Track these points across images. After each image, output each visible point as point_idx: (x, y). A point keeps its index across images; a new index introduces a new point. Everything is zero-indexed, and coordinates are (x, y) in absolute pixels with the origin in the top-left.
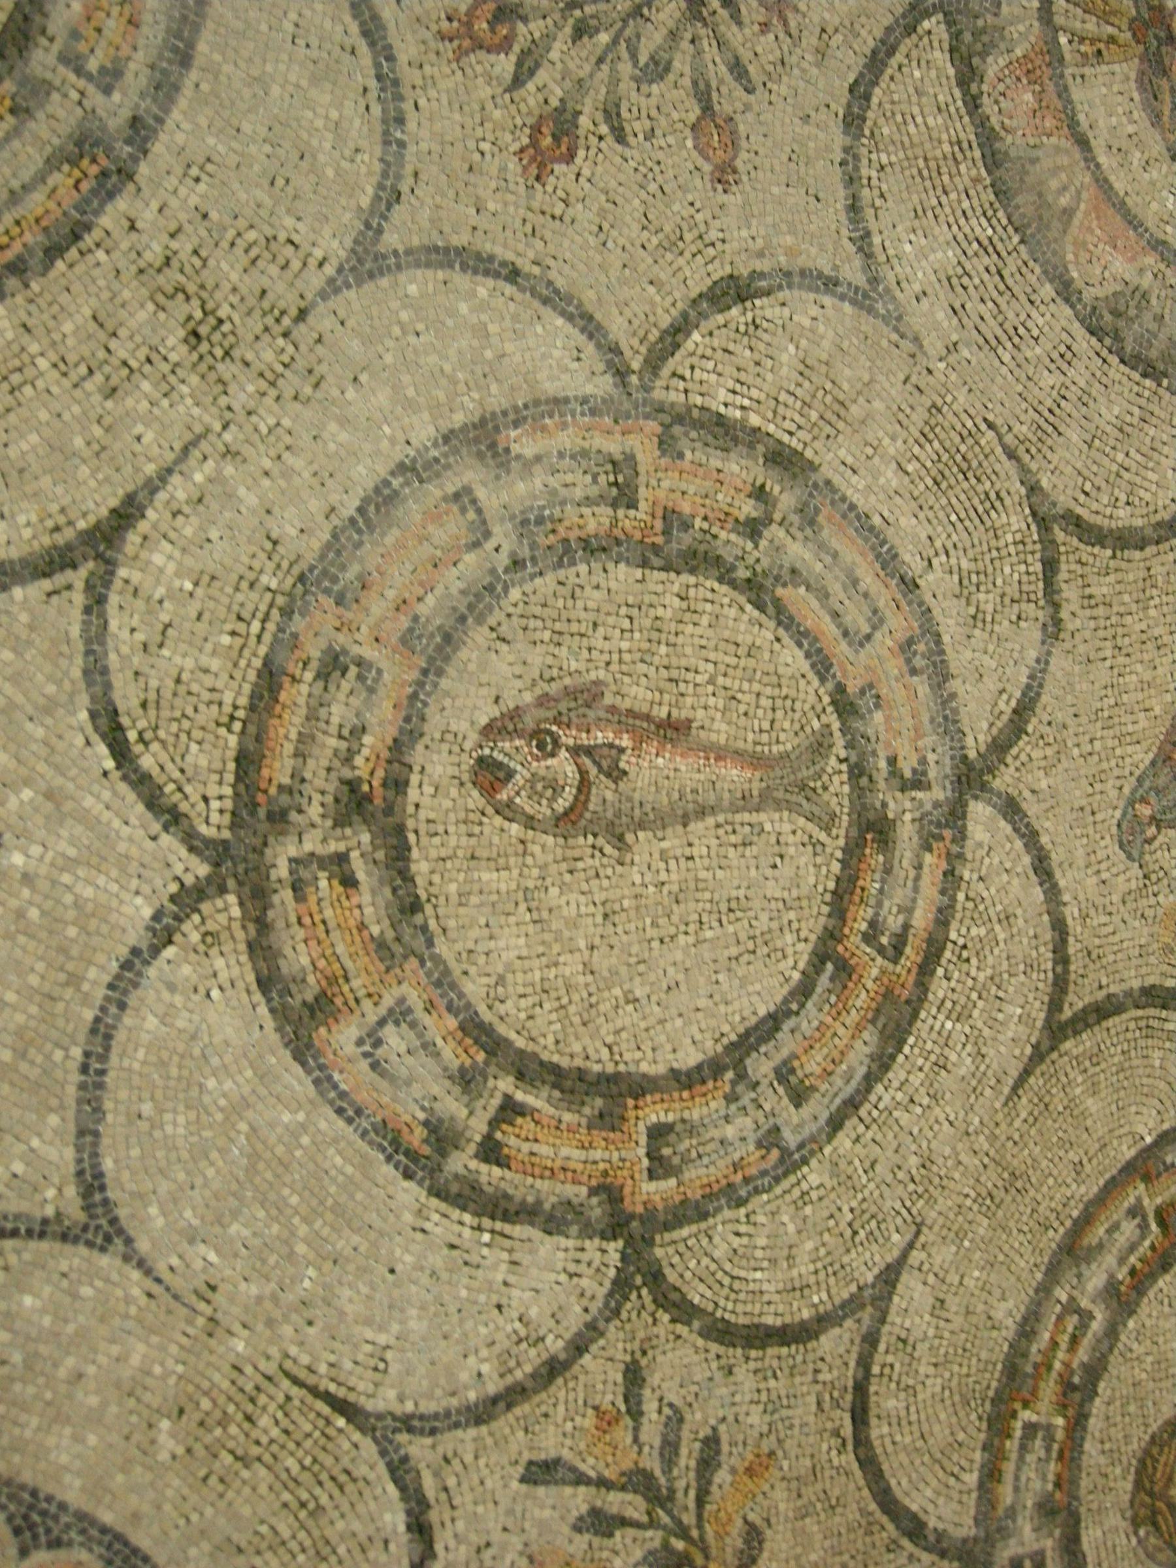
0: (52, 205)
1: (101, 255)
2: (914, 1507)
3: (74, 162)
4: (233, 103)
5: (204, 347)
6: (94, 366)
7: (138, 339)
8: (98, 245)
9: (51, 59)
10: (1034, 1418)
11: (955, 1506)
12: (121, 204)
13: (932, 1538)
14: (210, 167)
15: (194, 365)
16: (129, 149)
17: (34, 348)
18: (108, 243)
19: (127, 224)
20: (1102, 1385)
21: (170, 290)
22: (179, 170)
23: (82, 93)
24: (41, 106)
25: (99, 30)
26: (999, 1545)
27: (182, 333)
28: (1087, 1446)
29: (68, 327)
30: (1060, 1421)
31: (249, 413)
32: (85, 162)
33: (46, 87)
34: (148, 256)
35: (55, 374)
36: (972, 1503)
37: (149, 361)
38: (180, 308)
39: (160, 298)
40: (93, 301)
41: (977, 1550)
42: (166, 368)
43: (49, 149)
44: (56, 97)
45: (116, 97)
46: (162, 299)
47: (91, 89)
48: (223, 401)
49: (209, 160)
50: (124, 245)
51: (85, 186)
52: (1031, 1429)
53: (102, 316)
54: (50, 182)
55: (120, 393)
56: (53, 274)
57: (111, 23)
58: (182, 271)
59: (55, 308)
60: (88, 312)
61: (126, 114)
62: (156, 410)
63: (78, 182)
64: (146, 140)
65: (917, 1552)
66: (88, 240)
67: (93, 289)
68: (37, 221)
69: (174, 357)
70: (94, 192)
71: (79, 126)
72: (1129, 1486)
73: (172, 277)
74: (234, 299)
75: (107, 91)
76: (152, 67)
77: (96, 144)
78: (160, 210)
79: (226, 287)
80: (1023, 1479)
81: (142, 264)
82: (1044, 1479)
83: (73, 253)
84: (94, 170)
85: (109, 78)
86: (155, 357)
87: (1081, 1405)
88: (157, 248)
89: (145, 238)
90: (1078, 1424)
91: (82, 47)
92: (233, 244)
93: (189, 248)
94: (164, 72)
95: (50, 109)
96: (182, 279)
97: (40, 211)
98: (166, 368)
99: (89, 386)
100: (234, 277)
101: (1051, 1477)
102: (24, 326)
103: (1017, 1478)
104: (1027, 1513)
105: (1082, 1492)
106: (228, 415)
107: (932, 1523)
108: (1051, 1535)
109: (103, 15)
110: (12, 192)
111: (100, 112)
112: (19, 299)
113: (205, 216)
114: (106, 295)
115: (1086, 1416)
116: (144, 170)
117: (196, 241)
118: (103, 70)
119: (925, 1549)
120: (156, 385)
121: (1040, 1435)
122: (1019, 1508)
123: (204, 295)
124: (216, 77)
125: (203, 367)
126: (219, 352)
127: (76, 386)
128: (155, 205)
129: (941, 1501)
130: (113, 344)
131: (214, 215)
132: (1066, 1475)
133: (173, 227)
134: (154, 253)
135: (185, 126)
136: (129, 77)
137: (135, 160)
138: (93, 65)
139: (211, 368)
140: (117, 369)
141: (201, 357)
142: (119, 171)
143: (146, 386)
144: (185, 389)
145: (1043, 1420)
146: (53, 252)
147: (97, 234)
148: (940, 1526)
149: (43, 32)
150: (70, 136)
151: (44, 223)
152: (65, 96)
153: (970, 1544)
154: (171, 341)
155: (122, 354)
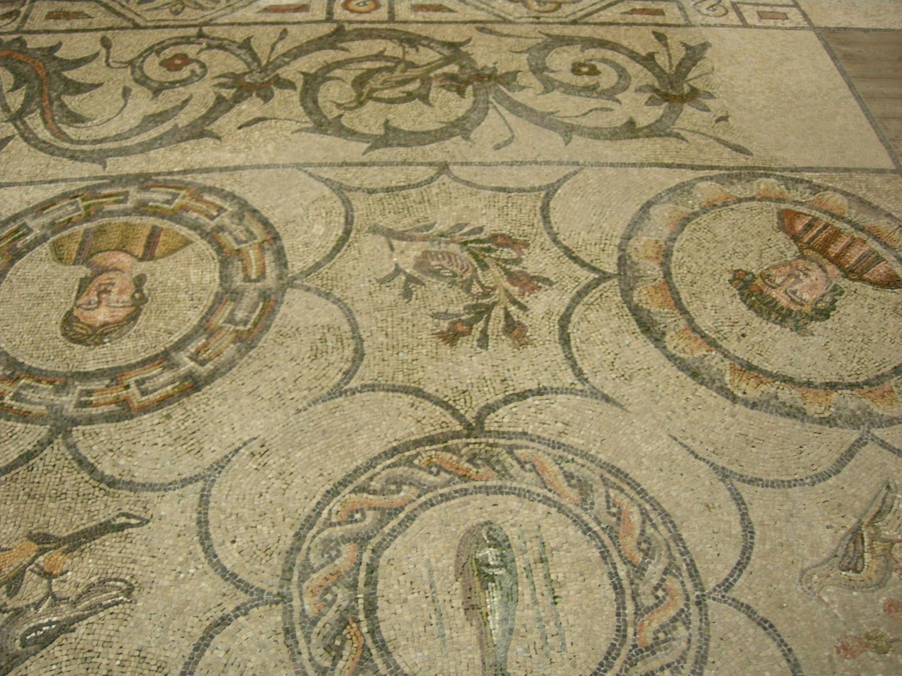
2: (16, 456)
10: (11, 394)
11: (27, 436)
13: (38, 448)
20: (21, 360)
26: (64, 413)
28: (44, 368)
30: (23, 381)
36: (33, 426)
41: (59, 424)
52: (17, 397)
65: (41, 456)
72: (79, 346)
80: (37, 400)
82: (44, 389)
87: (23, 370)
90: (30, 372)
101: (46, 386)
103: (35, 404)
104: (56, 398)
105: (66, 370)
107: (30, 448)
108: (76, 387)
115: (30, 367)
119: (42, 451)
121: (21, 391)
122: (51, 403)
129: (21, 443)
132: (49, 379)
145: (15, 390)
148: (35, 443)
153: (54, 429)
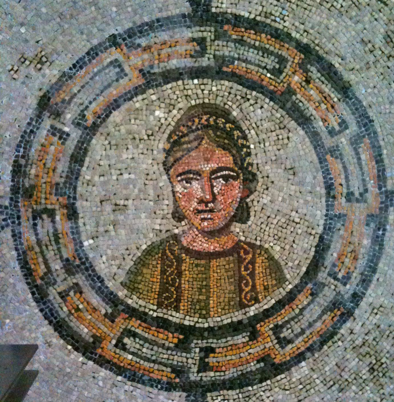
0: (323, 326)
1: (340, 343)
3: (332, 311)
4: (391, 285)
5: (375, 373)
6: (336, 381)
7: (352, 371)
8: (339, 340)
9: (325, 275)
12: (348, 324)
14: (381, 309)
15: (372, 379)
16: (352, 304)
17: (315, 376)
18: (343, 339)
19: (349, 331)
21: (364, 353)
22: (370, 311)
23: (336, 286)
24: (321, 291)
25: (343, 263)
27: (368, 369)
29: (327, 369)
31: (391, 395)
32: (336, 310)
33: (324, 285)
34: (357, 342)
35: (322, 385)
37: (355, 379)
38: (368, 360)
39: (361, 357)
40: (336, 359)
42: (361, 381)
43: (323, 308)
44: (326, 288)
45: (348, 286)
46: (362, 356)
47: (339, 284)
48: (382, 391)
49: (381, 306)
50: (349, 339)
51: (335, 319)
53: (339, 364)
54: (324, 318)
55: (344, 391)
56: (322, 351)
57: (347, 260)
58: (369, 347)
59: (323, 362)
60: (334, 363)
61: (351, 292)
62: (357, 396)
63: (333, 317)
64: (358, 301)
66: (336, 338)
67: (336, 355)
68: (318, 332)
69: (364, 377)
70: (338, 321)
71: (335, 298)
73: (366, 349)
74: (388, 355)
75: (345, 284)
76: (362, 274)
77: (340, 304)
78: (362, 326)
79: (385, 351)
81: (354, 345)
83: (330, 343)
84: (339, 313)
85: (346, 280)
86: (357, 377)
88: (360, 339)
89: (356, 336)
91: (336, 269)
92: (388, 336)
93: (372, 338)
94: (366, 276)
95: (324, 293)
96: (369, 349)
97: (319, 329)
98: (361, 381)
99: (333, 388)
100: (388, 348)
102: (312, 369)
106: (383, 396)
109: (344, 257)
110: (310, 323)
111: (342, 293)
112: (311, 360)
113: (378, 327)
114: (341, 357)
116: (357, 312)
117: (374, 335)
118: (344, 277)
120: (357, 387)
123: (377, 355)
124: (385, 275)
125: (375, 380)
126: (381, 375)
127: (329, 389)
128: (360, 324)
130: (343, 374)
131: (382, 326)
133: (366, 332)
134: (359, 342)
135: (373, 295)
136: (353, 279)
137: (354, 308)
138: (340, 276)
139: (377, 380)
140: (343, 382)
141: (374, 377)
142: (348, 312)
143: (354, 388)
144: (368, 388)
146: (323, 343)
147: (339, 336)
149: (323, 265)
150: (331, 301)
151: (320, 333)
152: (330, 288)
154: (364, 372)
155: (346, 377)
